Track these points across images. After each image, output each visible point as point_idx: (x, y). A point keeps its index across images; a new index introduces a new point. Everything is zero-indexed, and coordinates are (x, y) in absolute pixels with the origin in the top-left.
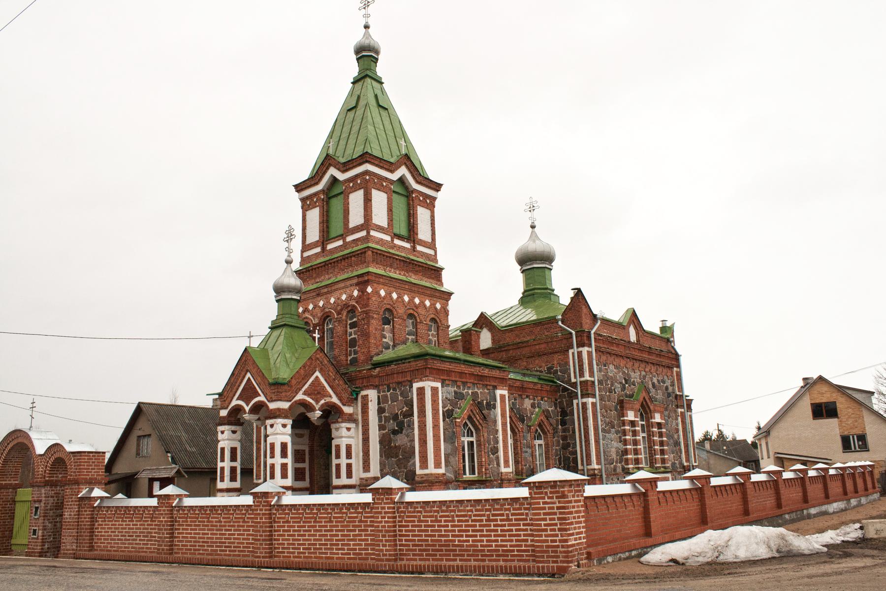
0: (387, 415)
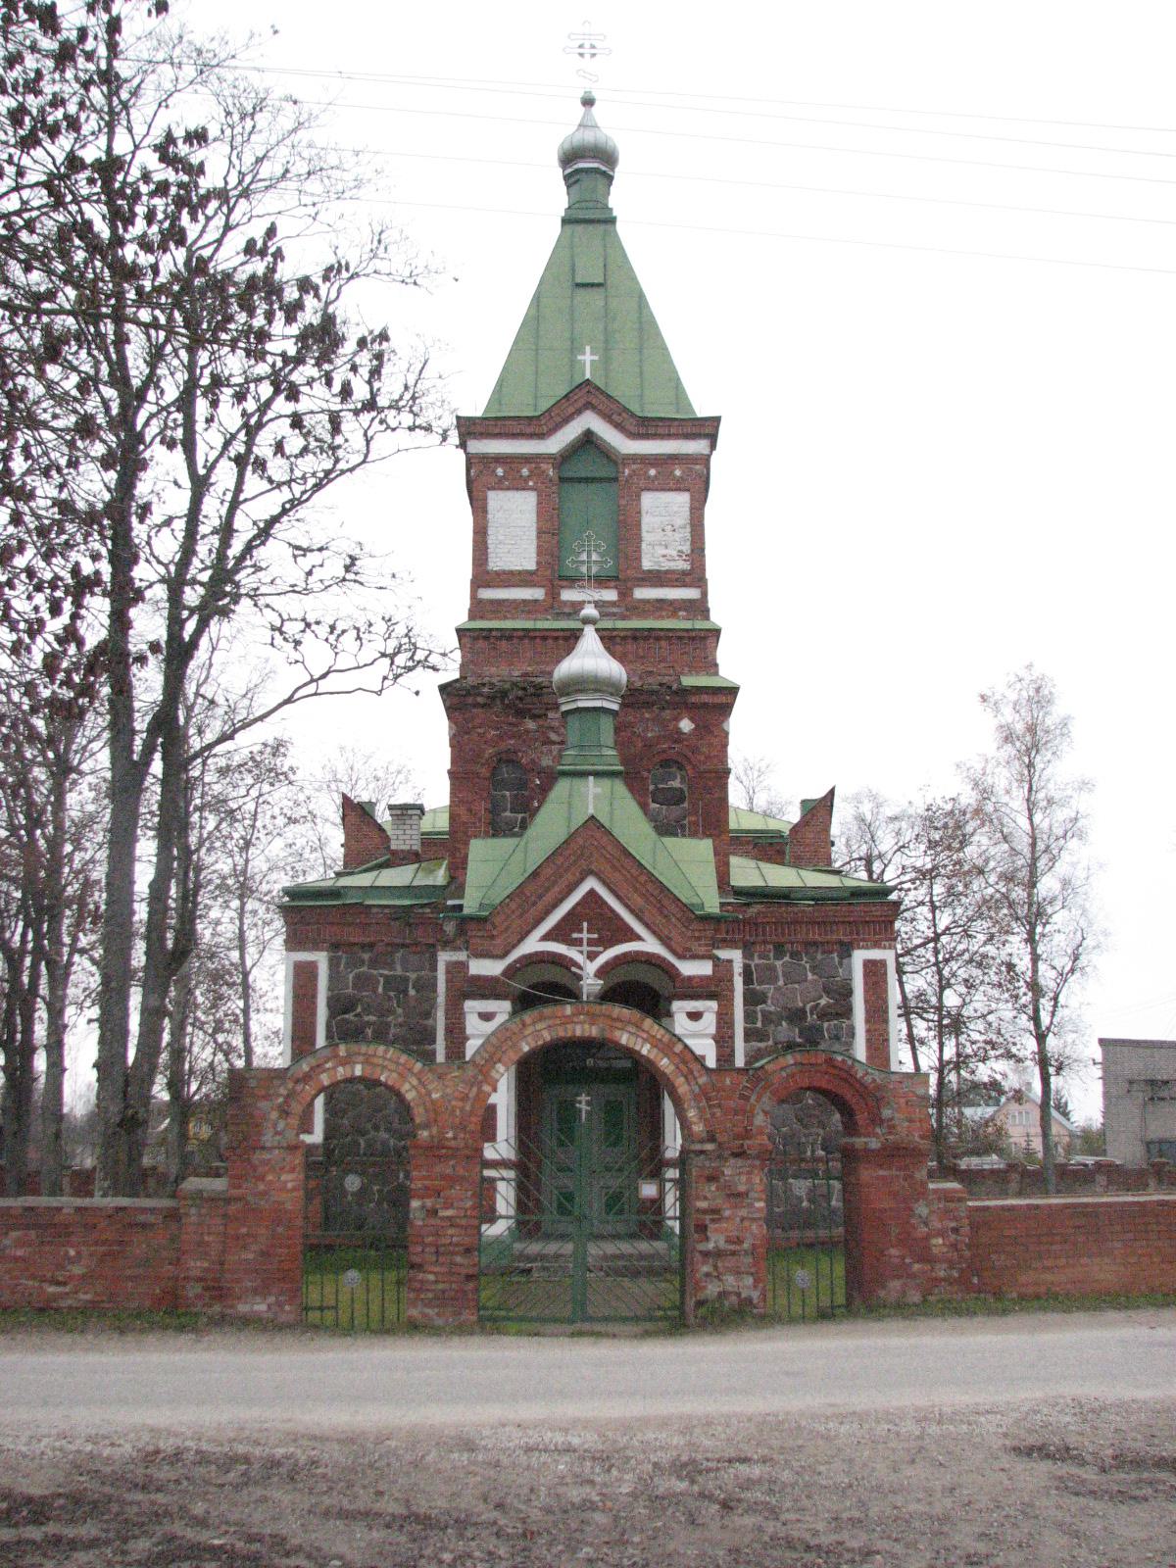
0: (772, 1009)
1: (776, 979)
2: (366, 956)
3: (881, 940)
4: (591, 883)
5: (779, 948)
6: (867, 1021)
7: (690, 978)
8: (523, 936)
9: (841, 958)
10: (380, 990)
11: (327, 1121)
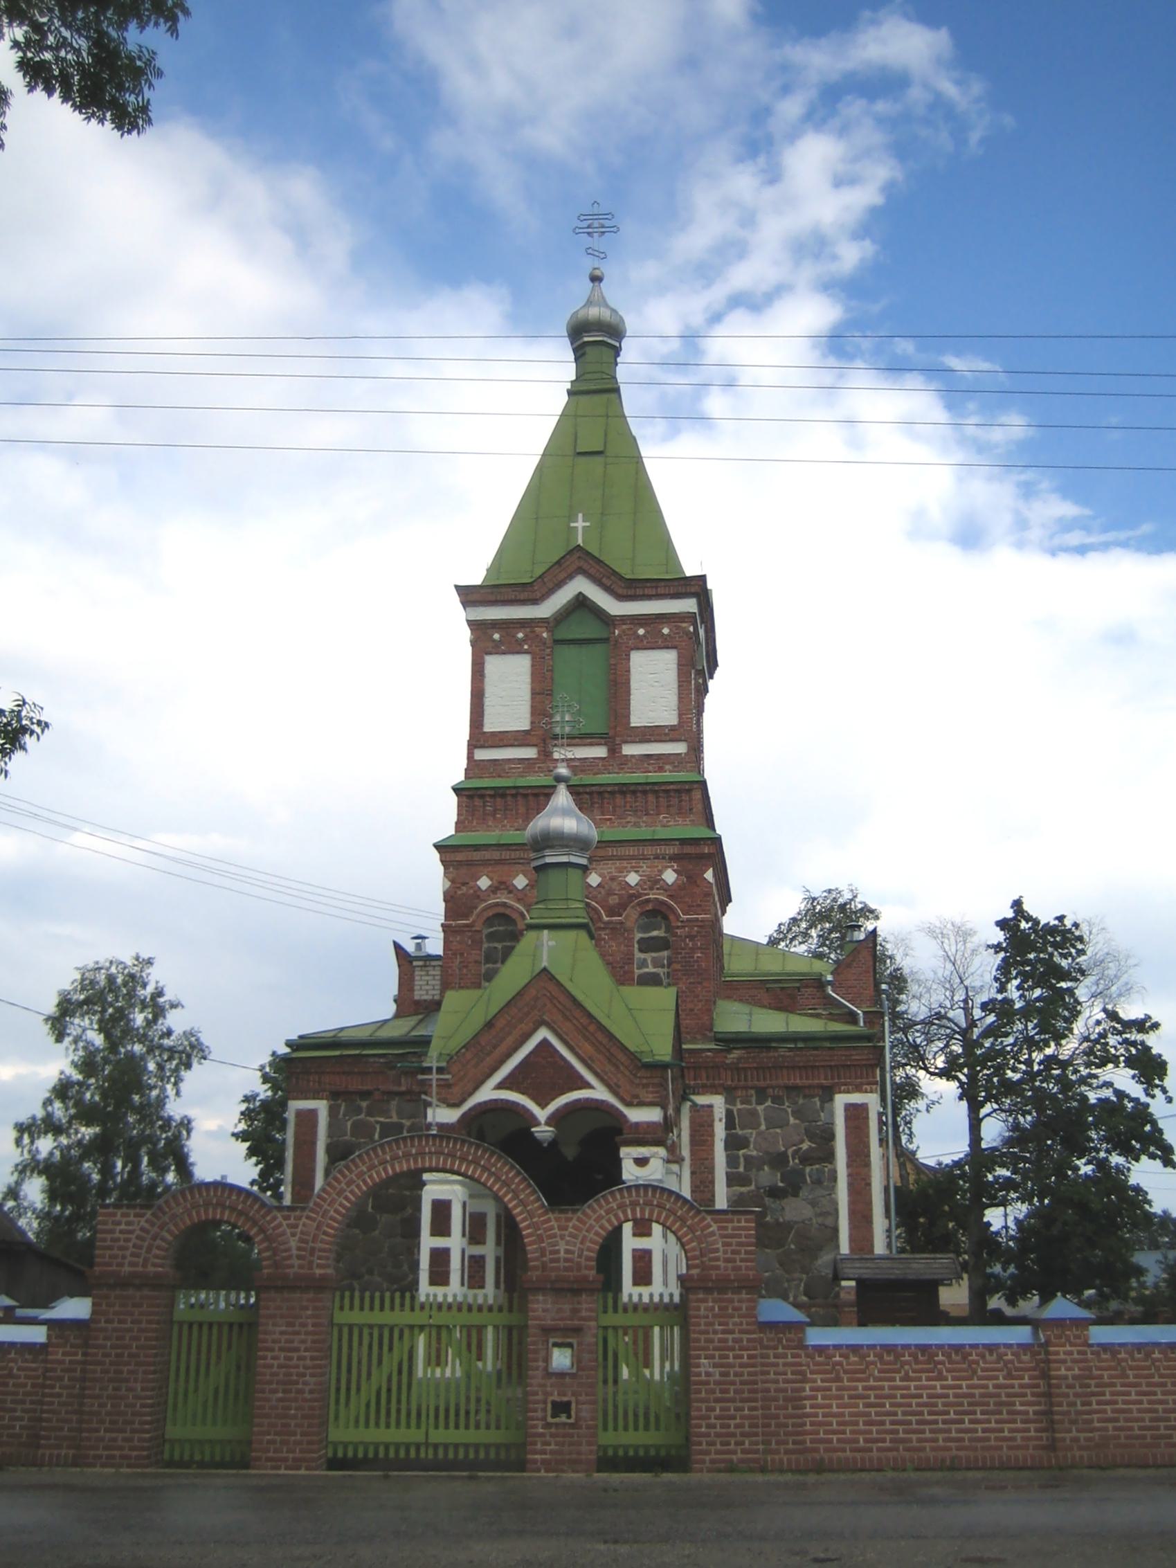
0: (754, 1153)
1: (759, 1125)
2: (364, 1104)
3: (862, 1084)
4: (543, 1033)
5: (762, 1095)
6: (849, 1166)
7: (637, 1124)
8: (477, 1087)
9: (823, 1102)
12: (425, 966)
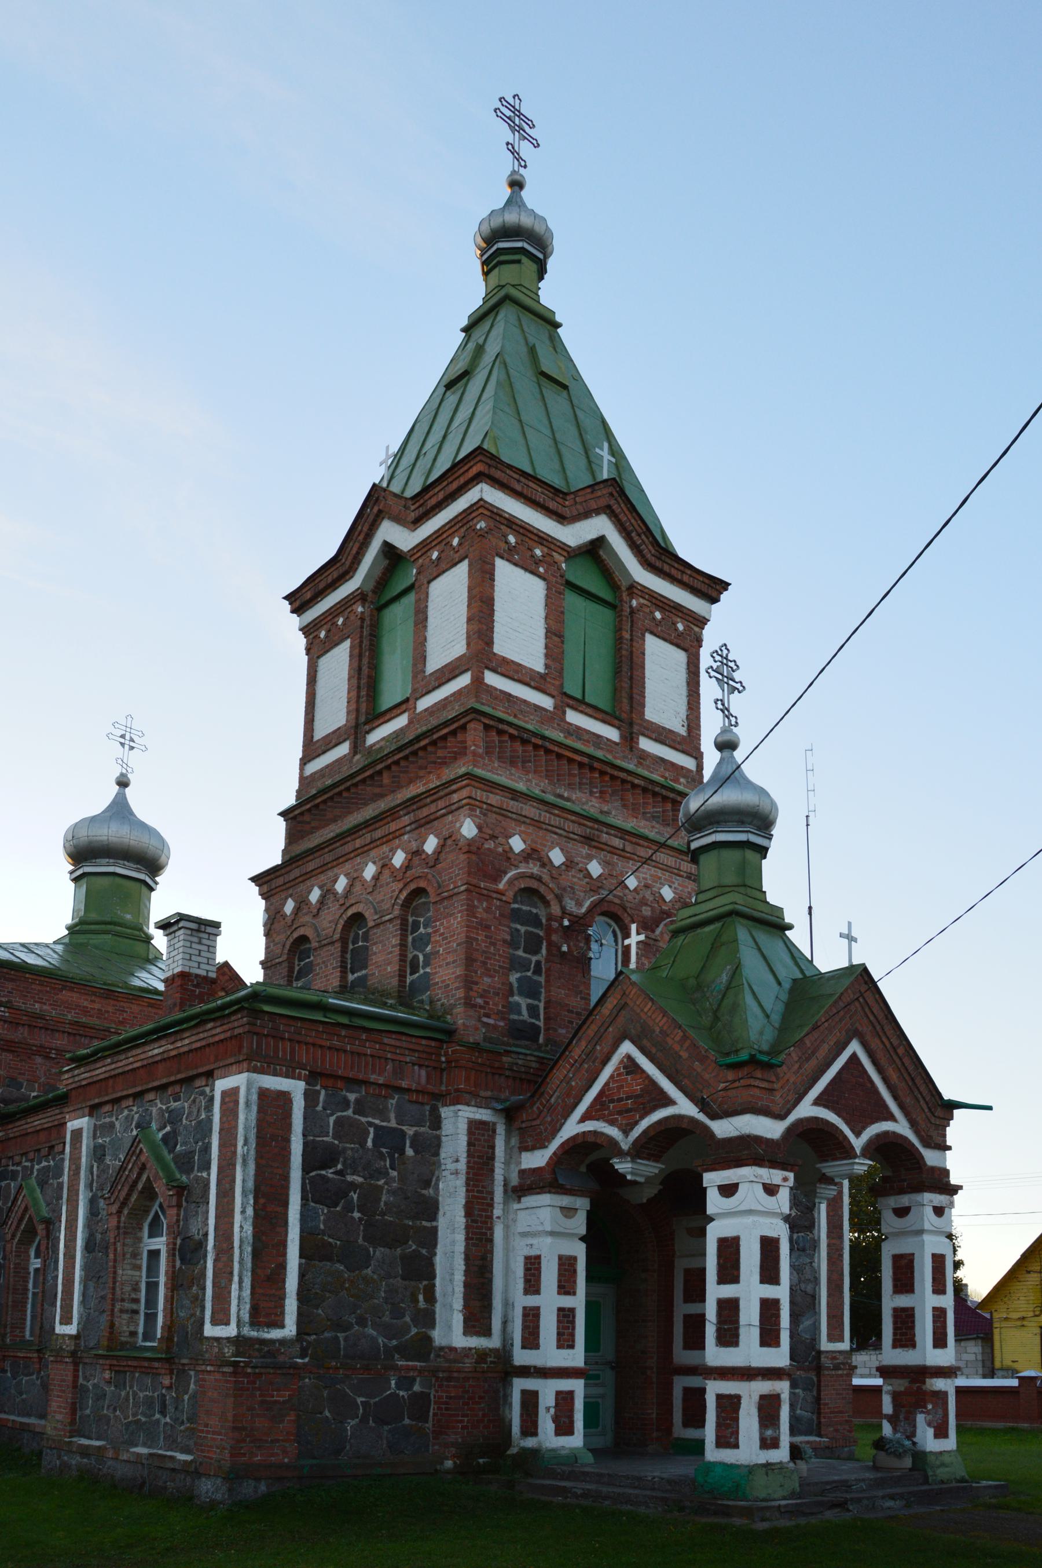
2: (352, 1097)
10: (370, 1143)
11: (300, 1314)
12: (198, 931)
